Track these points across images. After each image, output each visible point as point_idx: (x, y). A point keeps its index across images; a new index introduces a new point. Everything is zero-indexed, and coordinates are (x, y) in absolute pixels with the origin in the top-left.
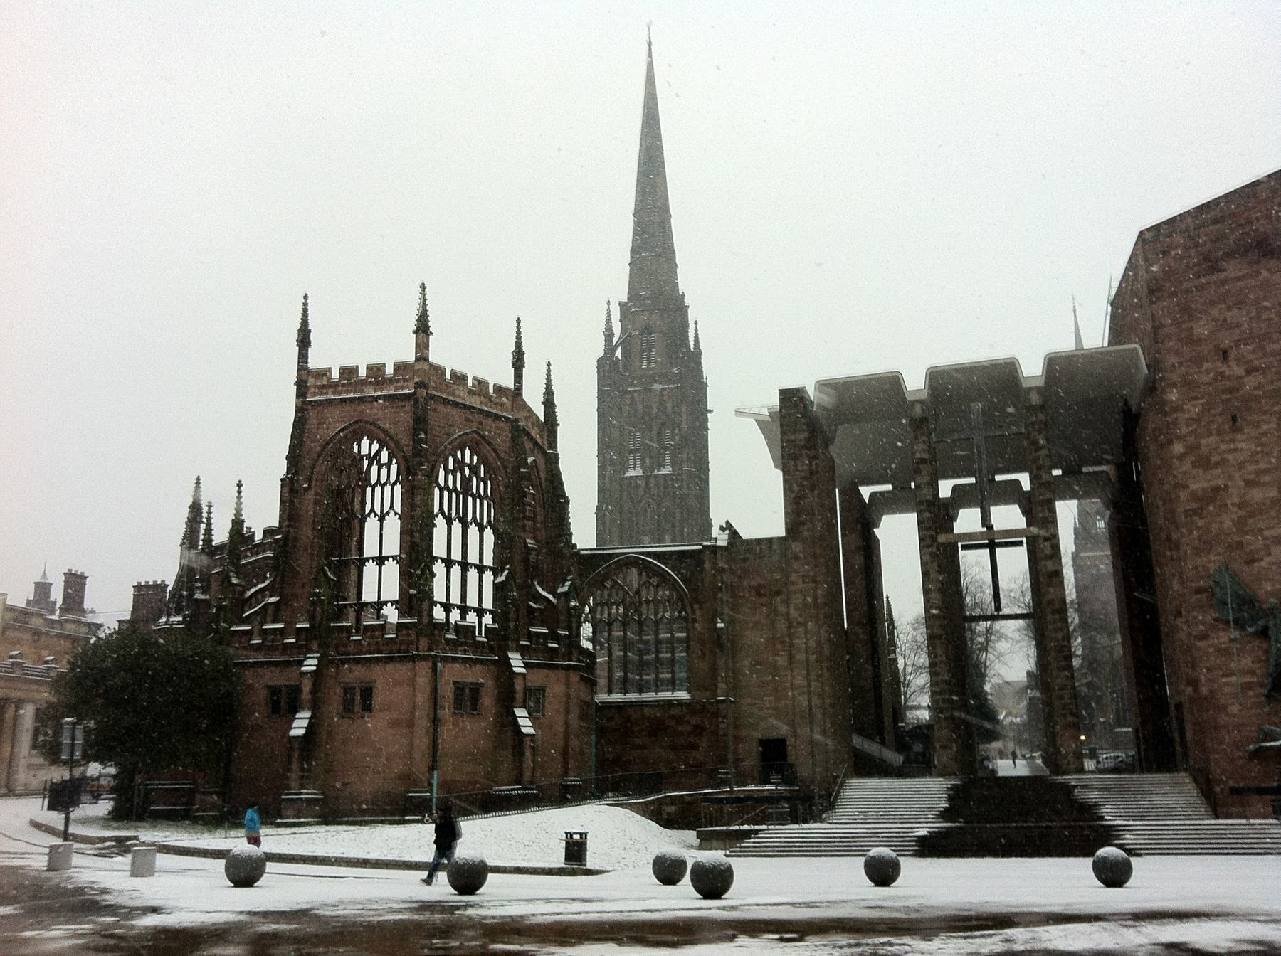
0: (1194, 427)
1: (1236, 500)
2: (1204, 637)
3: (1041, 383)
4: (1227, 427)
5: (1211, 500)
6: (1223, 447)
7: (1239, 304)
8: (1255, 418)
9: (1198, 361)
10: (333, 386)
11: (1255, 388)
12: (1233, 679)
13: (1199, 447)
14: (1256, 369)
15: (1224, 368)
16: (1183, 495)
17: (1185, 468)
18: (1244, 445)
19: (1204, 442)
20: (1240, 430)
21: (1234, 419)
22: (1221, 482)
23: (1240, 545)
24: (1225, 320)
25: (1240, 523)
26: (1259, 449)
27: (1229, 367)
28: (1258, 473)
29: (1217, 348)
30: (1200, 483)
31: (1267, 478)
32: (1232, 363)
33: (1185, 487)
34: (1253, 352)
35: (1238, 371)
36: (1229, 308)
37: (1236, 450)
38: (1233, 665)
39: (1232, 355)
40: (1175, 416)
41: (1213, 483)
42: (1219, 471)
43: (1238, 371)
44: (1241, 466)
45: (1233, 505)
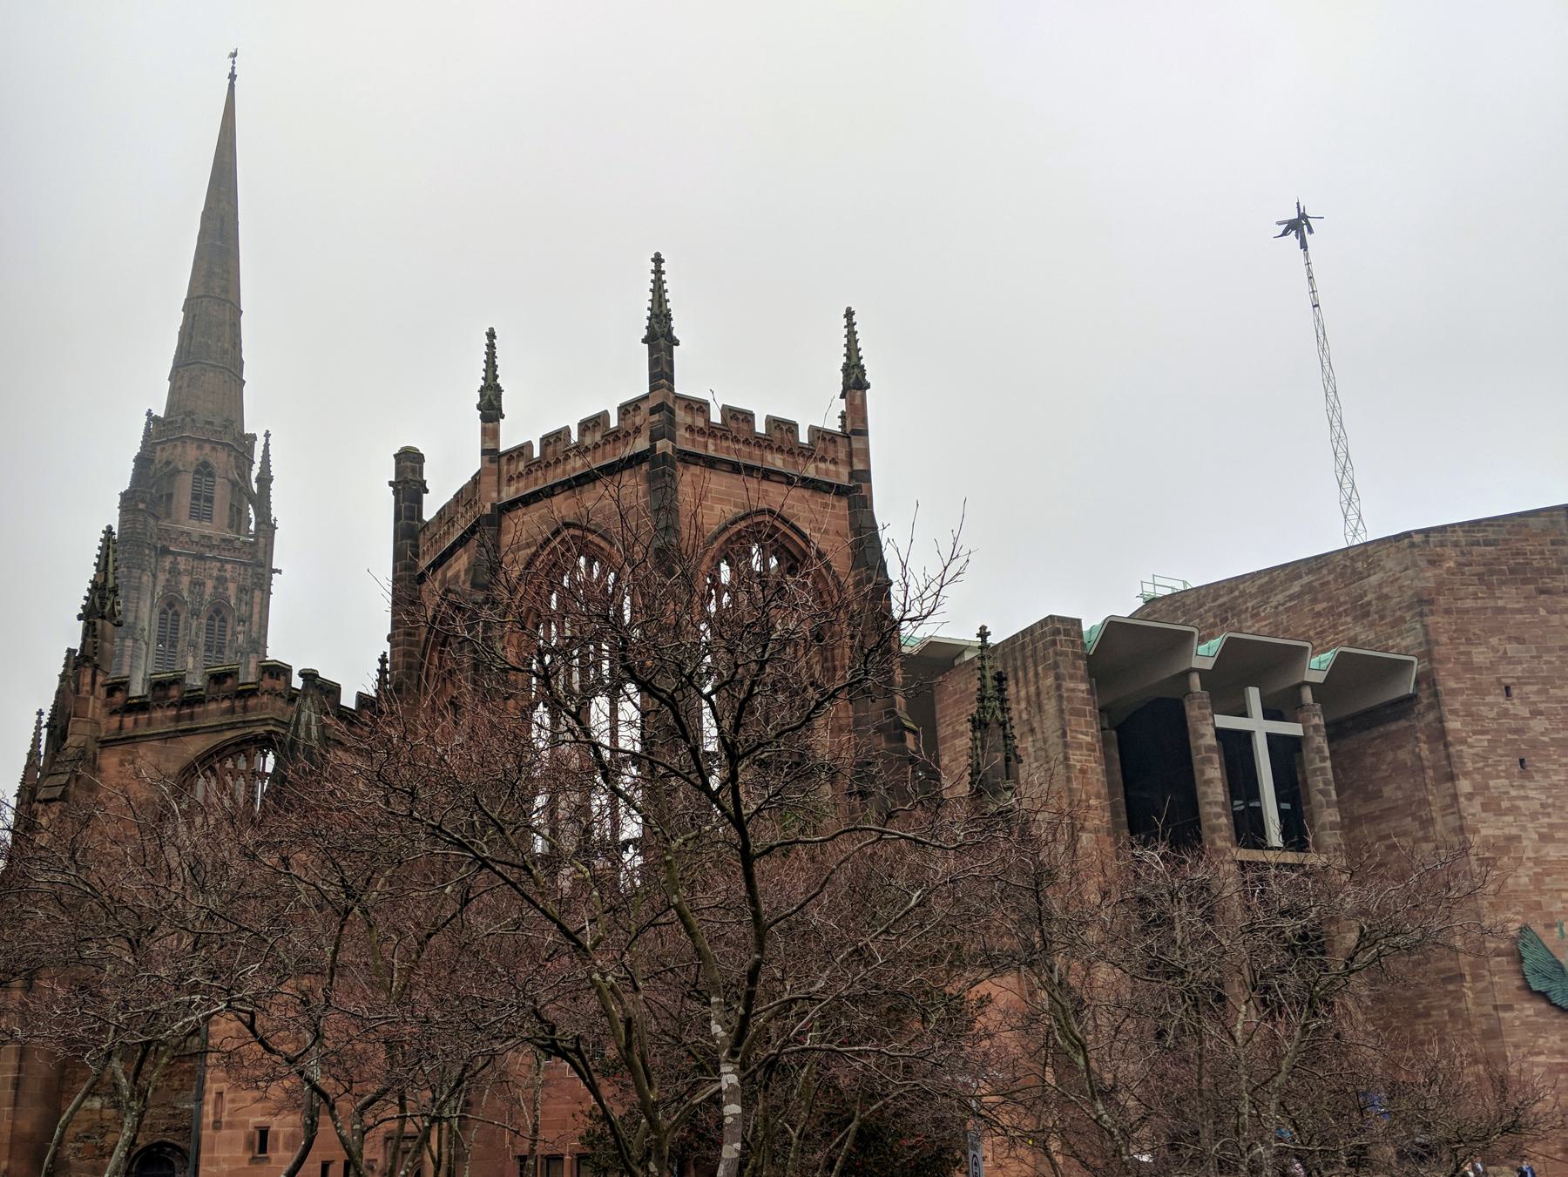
0: (1482, 764)
1: (1532, 855)
2: (1509, 1008)
3: (1319, 678)
4: (1516, 770)
5: (1505, 850)
6: (1513, 793)
7: (1520, 640)
8: (1544, 765)
9: (1480, 691)
10: (711, 431)
11: (1542, 734)
12: (1542, 1059)
13: (1487, 787)
14: (1541, 713)
15: (1508, 705)
16: (1475, 840)
17: (1472, 811)
18: (1536, 794)
19: (1492, 783)
20: (1530, 778)
21: (1522, 761)
22: (1514, 831)
23: (1539, 904)
24: (1505, 652)
25: (1537, 879)
26: (1550, 801)
27: (1513, 704)
28: (1551, 826)
29: (1498, 679)
30: (1490, 829)
31: (1559, 835)
32: (1515, 701)
33: (1476, 831)
34: (1538, 693)
35: (1524, 712)
36: (1510, 639)
37: (1526, 798)
38: (1541, 1041)
39: (1515, 692)
40: (1459, 748)
41: (1507, 831)
42: (1510, 819)
43: (1524, 712)
44: (1534, 816)
45: (1528, 859)
